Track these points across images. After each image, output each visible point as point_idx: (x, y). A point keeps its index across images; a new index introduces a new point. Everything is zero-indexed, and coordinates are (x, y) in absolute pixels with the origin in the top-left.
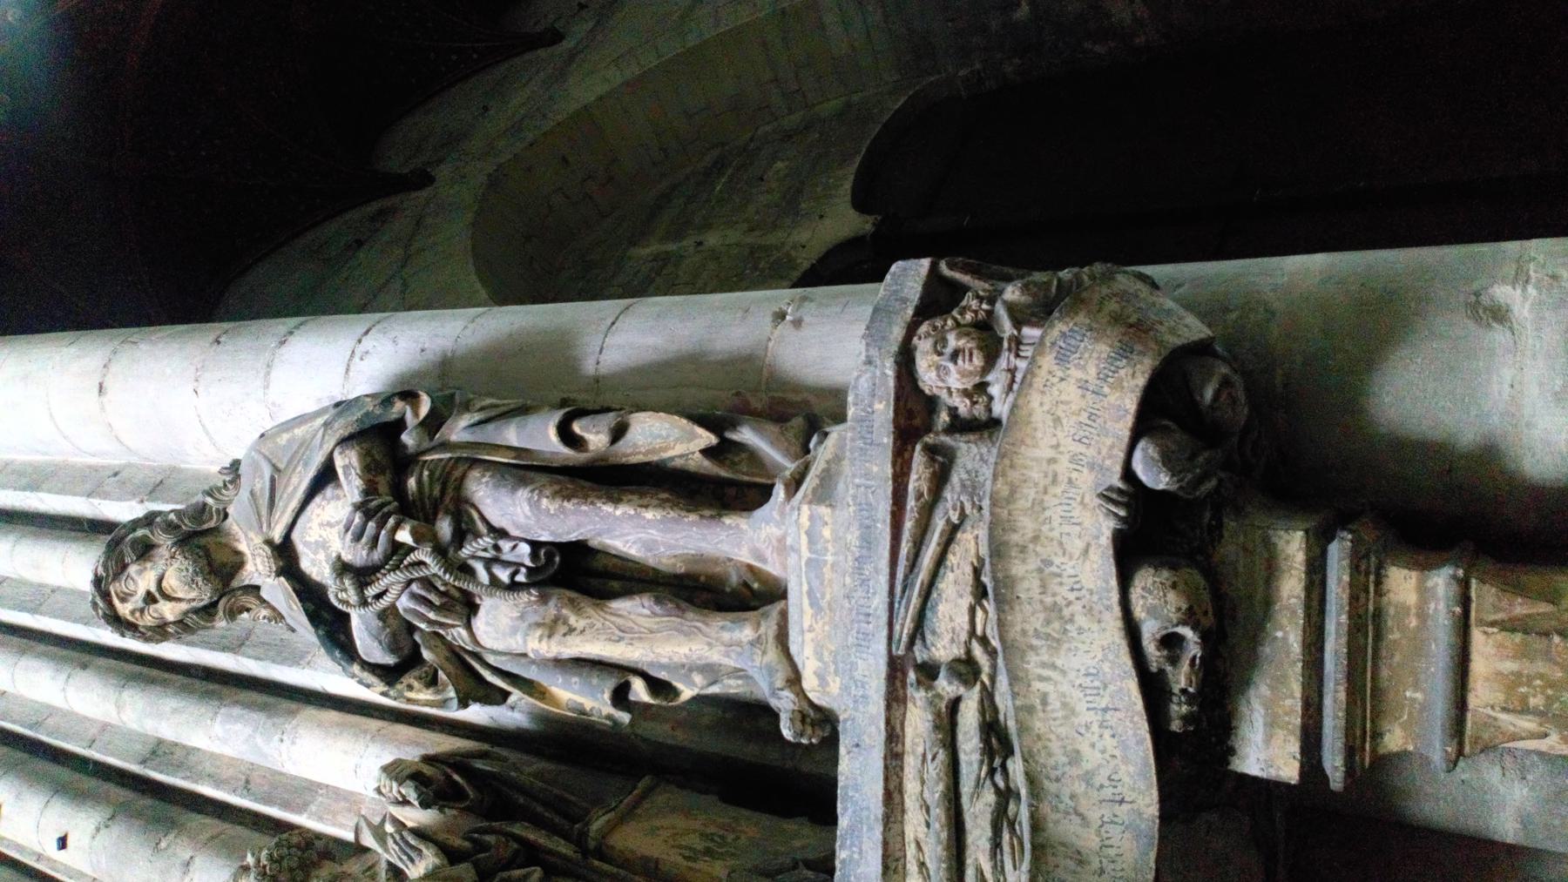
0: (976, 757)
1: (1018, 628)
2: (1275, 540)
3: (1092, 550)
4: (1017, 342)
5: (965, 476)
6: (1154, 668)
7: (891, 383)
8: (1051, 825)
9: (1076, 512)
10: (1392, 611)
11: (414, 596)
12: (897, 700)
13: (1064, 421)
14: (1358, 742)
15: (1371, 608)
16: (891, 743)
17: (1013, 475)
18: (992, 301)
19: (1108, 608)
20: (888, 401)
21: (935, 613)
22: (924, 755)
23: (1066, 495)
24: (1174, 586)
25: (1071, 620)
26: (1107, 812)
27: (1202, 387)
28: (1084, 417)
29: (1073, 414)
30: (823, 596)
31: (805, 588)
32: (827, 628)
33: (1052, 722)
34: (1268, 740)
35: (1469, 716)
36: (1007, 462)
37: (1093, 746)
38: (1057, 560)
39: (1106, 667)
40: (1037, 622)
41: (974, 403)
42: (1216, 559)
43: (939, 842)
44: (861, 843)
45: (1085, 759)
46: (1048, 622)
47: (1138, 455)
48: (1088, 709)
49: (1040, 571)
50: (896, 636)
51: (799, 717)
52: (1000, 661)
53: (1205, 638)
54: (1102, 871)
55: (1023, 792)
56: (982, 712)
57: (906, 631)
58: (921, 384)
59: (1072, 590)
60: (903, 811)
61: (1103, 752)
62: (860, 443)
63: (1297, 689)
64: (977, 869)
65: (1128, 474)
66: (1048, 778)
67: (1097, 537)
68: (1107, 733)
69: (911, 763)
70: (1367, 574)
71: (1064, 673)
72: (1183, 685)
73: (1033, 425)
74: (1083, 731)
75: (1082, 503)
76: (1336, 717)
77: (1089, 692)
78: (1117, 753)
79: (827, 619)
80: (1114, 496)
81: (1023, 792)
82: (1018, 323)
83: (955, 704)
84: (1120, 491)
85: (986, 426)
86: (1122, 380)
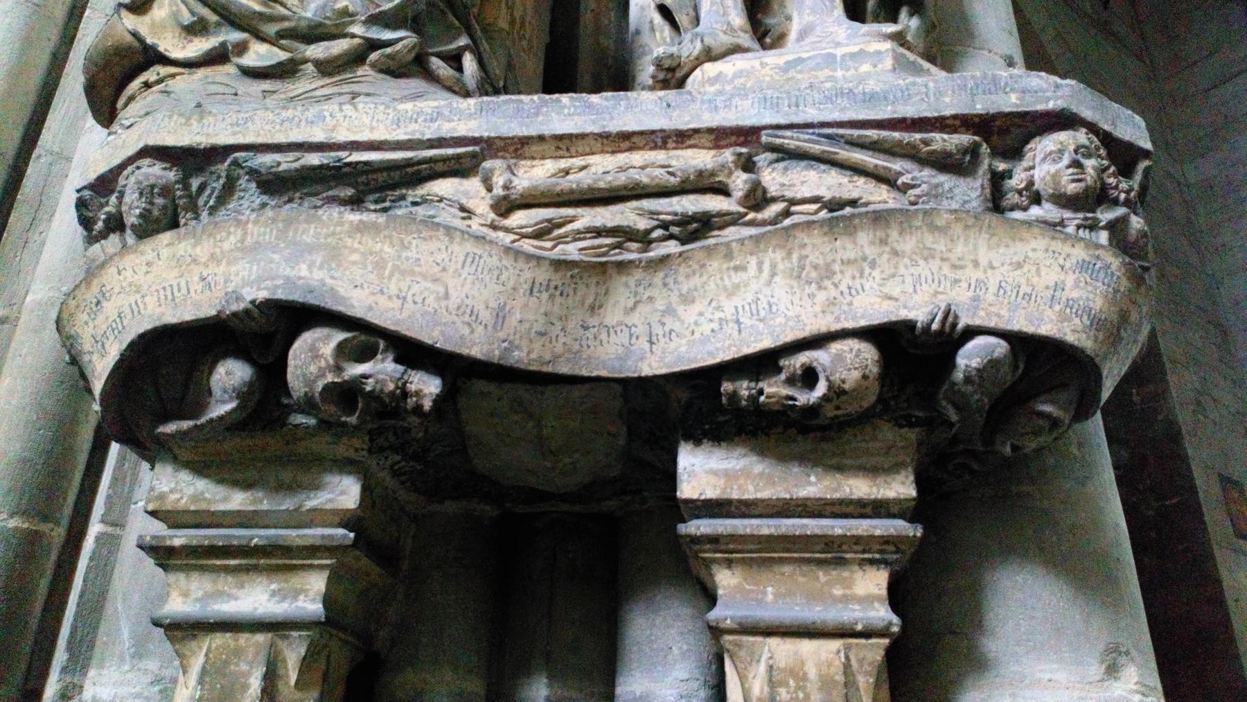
0: (679, 209)
1: (806, 241)
2: (903, 473)
3: (892, 303)
4: (1093, 227)
5: (946, 186)
6: (782, 363)
7: (1040, 107)
8: (624, 279)
9: (927, 289)
10: (846, 574)
12: (717, 139)
13: (1018, 272)
14: (723, 547)
15: (848, 556)
16: (676, 135)
17: (957, 229)
18: (1127, 203)
19: (838, 319)
20: (1017, 106)
21: (806, 168)
22: (669, 166)
23: (942, 279)
24: (865, 377)
25: (820, 288)
26: (641, 330)
27: (1052, 402)
28: (1025, 289)
29: (1028, 280)
30: (800, 72)
31: (805, 55)
32: (768, 79)
33: (719, 277)
34: (715, 473)
35: (759, 639)
36: (971, 221)
37: (701, 314)
38: (876, 273)
39: (780, 320)
40: (814, 257)
41: (1020, 193)
42: (879, 422)
43: (596, 181)
44: (579, 114)
45: (687, 308)
46: (816, 267)
47: (992, 340)
48: (736, 307)
49: (864, 259)
50: (780, 133)
51: (675, 64)
52: (769, 228)
53: (812, 411)
54: (586, 328)
55: (651, 254)
56: (720, 214)
57: (786, 141)
58: (1037, 139)
59: (850, 288)
60: (613, 152)
61: (696, 323)
62: (971, 84)
63: (765, 494)
64: (575, 217)
65: (972, 332)
66: (666, 276)
67: (905, 307)
68: (715, 326)
69: (660, 156)
70: (881, 552)
71: (769, 283)
72: (768, 390)
73: (1011, 243)
74: (713, 304)
75: (936, 293)
76: (746, 527)
77: (754, 306)
78: (697, 335)
79: (778, 78)
80: (950, 319)
81: (651, 254)
82: (1112, 226)
83: (723, 191)
84: (954, 325)
85: (996, 202)
86: (1069, 321)
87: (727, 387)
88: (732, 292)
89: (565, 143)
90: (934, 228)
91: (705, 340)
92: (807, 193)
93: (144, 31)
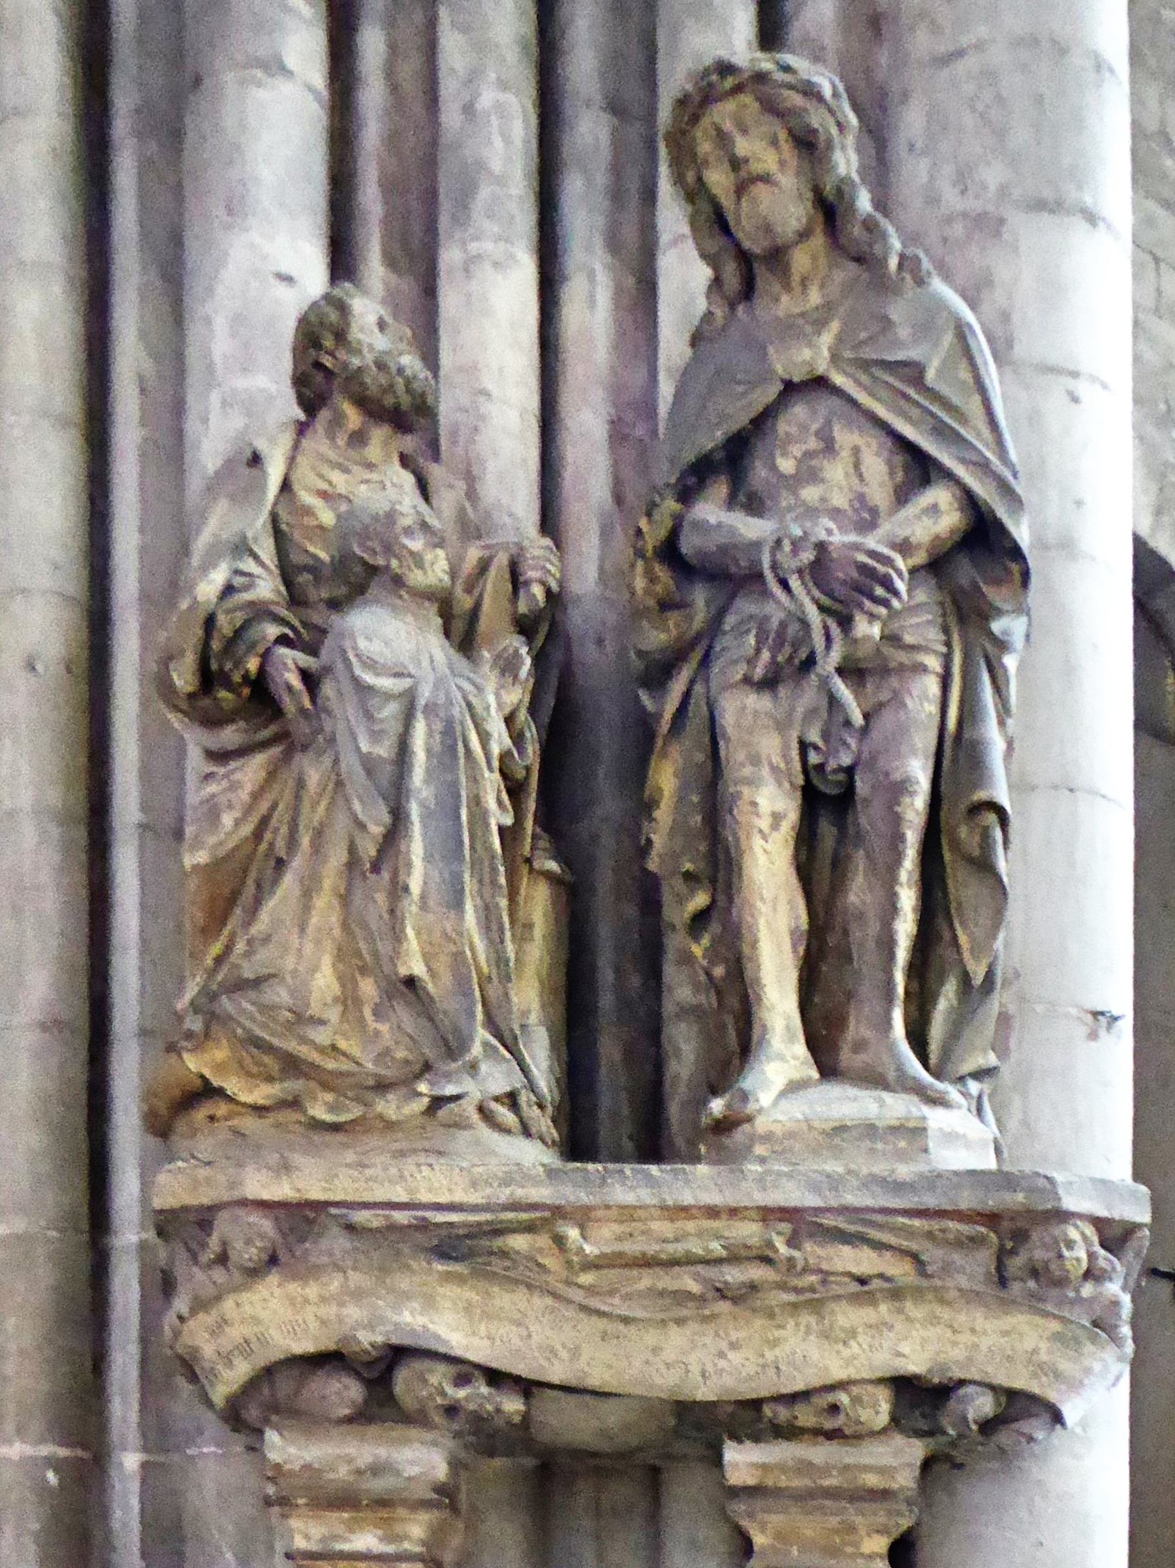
11: (783, 625)
87: (767, 1411)
88: (774, 1343)
89: (627, 1213)
90: (942, 1301)
91: (750, 1378)
92: (839, 1267)
93: (207, 1073)
